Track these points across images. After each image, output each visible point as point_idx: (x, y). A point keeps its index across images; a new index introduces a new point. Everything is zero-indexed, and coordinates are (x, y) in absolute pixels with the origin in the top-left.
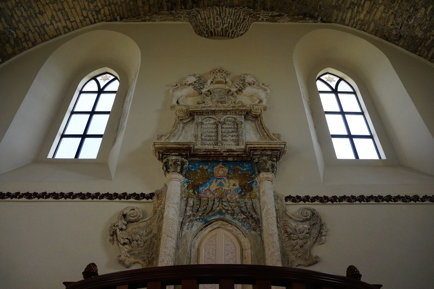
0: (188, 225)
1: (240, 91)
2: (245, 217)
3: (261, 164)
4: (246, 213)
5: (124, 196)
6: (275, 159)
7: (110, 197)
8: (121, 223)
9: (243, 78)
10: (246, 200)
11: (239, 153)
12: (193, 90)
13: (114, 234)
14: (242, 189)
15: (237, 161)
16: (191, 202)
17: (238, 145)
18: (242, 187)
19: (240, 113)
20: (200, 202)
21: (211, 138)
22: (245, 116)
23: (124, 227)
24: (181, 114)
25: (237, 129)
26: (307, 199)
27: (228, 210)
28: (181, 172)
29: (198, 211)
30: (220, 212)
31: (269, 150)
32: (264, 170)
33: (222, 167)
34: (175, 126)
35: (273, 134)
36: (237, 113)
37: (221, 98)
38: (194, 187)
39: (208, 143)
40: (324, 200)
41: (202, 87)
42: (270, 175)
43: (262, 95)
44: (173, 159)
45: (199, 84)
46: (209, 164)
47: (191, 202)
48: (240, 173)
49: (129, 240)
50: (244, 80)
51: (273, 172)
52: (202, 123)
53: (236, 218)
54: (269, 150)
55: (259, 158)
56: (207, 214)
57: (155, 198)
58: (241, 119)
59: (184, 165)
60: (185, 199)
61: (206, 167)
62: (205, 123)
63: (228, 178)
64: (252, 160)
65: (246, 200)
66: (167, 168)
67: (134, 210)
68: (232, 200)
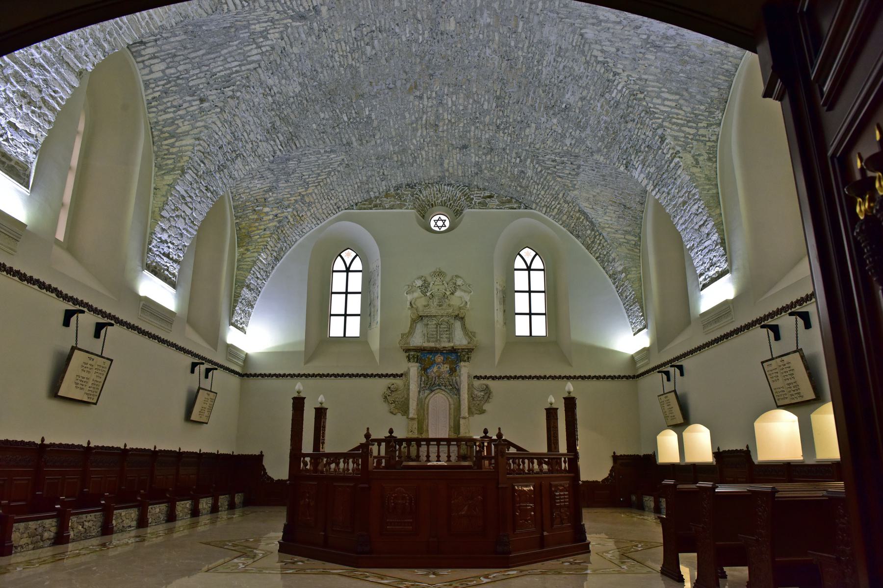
1: (452, 294)
5: (387, 376)
13: (385, 397)
17: (449, 341)
18: (451, 369)
26: (485, 378)
40: (494, 378)
42: (466, 364)
43: (467, 297)
58: (452, 321)
64: (457, 353)
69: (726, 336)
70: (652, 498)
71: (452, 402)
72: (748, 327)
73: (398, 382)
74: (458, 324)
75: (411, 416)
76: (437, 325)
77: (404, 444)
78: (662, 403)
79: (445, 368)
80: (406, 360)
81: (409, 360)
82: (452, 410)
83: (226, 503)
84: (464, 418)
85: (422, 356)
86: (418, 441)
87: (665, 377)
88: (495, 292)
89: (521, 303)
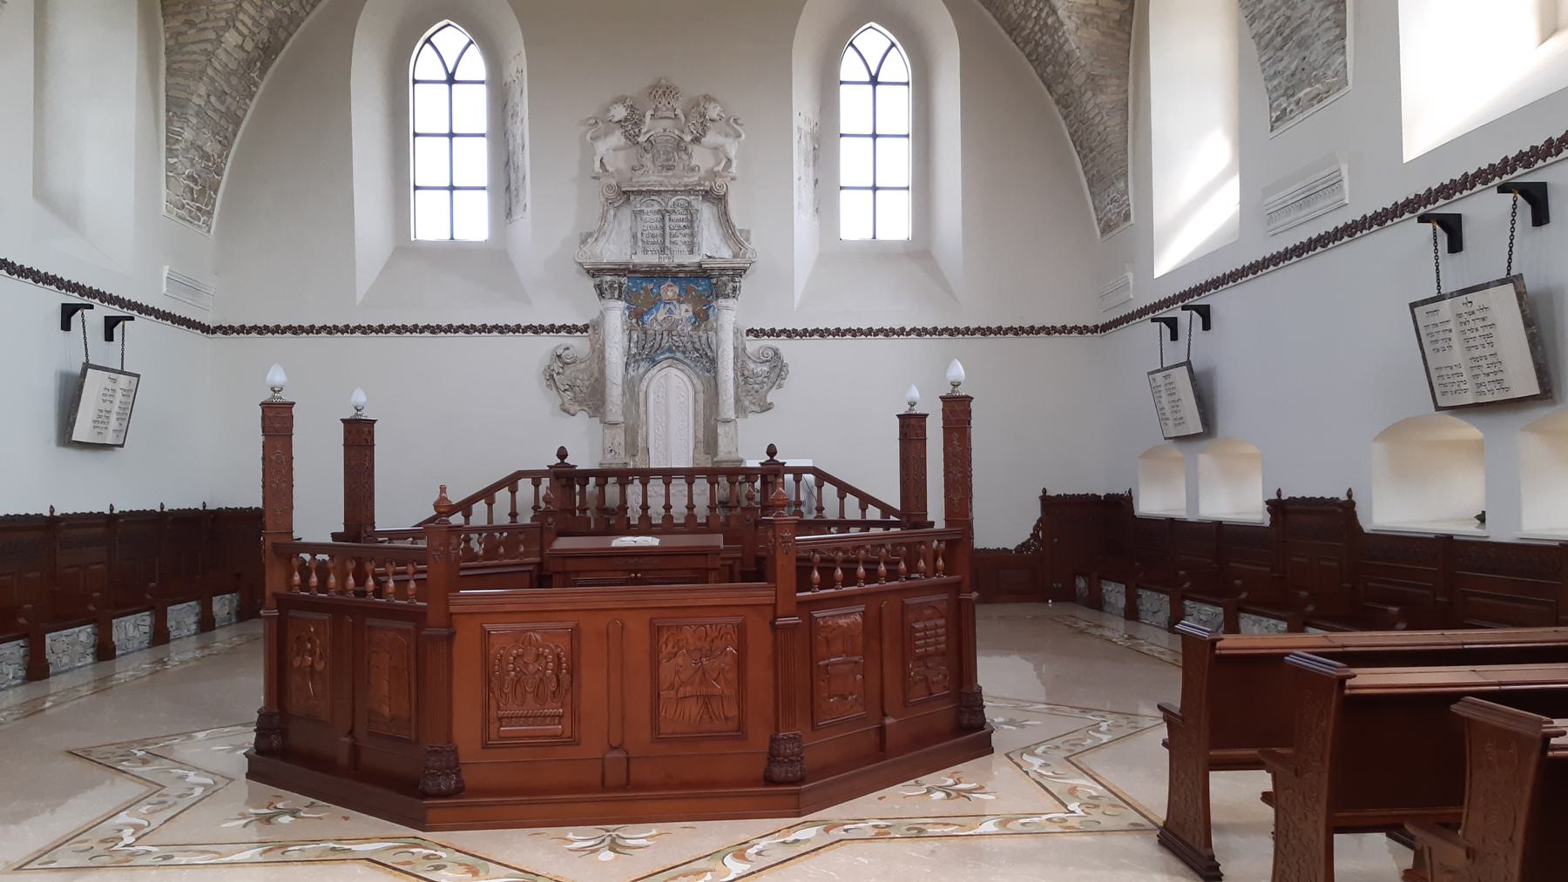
1: (696, 140)
5: (552, 329)
7: (537, 330)
8: (557, 366)
16: (635, 336)
24: (611, 195)
26: (773, 333)
28: (619, 298)
30: (670, 350)
34: (604, 218)
35: (741, 231)
39: (651, 247)
40: (791, 334)
42: (730, 302)
43: (732, 149)
45: (631, 125)
47: (635, 336)
50: (703, 115)
57: (590, 331)
61: (651, 286)
64: (709, 278)
69: (1323, 241)
70: (1122, 588)
71: (700, 387)
72: (1380, 219)
73: (579, 345)
74: (706, 212)
75: (611, 418)
76: (663, 214)
77: (592, 480)
78: (1155, 390)
79: (684, 312)
80: (594, 293)
81: (601, 294)
82: (701, 403)
83: (193, 619)
84: (727, 421)
85: (634, 284)
86: (624, 476)
87: (1167, 331)
88: (796, 136)
89: (853, 160)
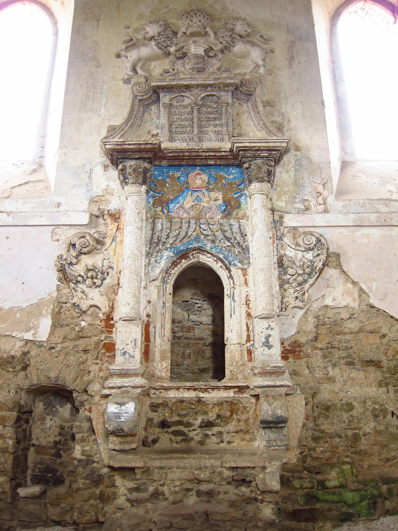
0: (156, 256)
2: (229, 244)
3: (253, 170)
4: (231, 239)
6: (273, 164)
9: (232, 26)
10: (232, 221)
11: (223, 154)
12: (155, 47)
14: (226, 206)
15: (220, 165)
18: (227, 202)
19: (226, 88)
20: (171, 225)
21: (184, 130)
22: (233, 92)
23: (74, 261)
25: (221, 114)
27: (207, 235)
29: (168, 238)
31: (265, 150)
32: (257, 179)
33: (200, 174)
36: (222, 88)
37: (198, 63)
38: (163, 203)
39: (180, 136)
41: (169, 43)
44: (132, 164)
46: (182, 169)
48: (224, 181)
49: (83, 277)
50: (232, 30)
51: (269, 181)
52: (171, 105)
53: (218, 246)
54: (265, 150)
55: (251, 161)
56: (181, 241)
59: (147, 173)
60: (151, 220)
61: (178, 174)
62: (175, 103)
63: (208, 189)
65: (232, 221)
66: (125, 178)
67: (84, 237)
68: (212, 222)
